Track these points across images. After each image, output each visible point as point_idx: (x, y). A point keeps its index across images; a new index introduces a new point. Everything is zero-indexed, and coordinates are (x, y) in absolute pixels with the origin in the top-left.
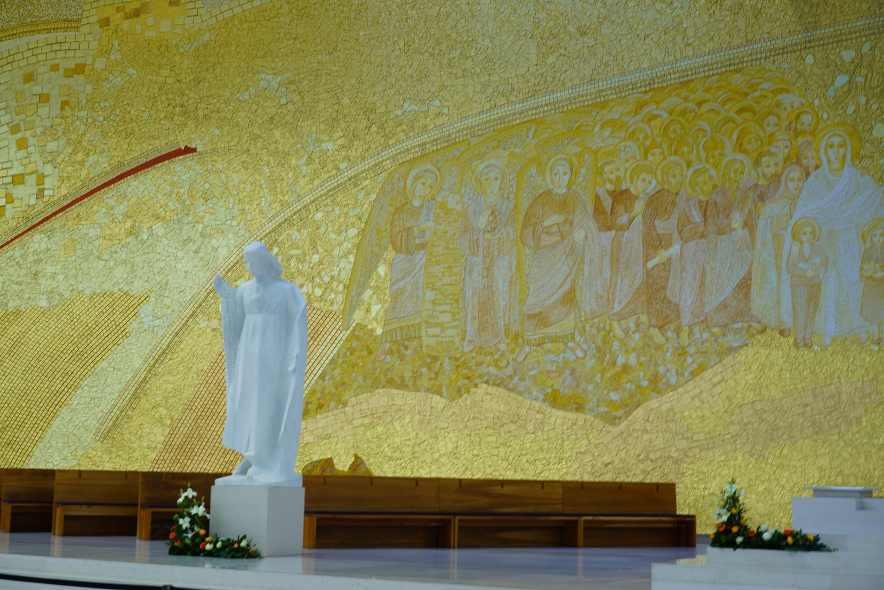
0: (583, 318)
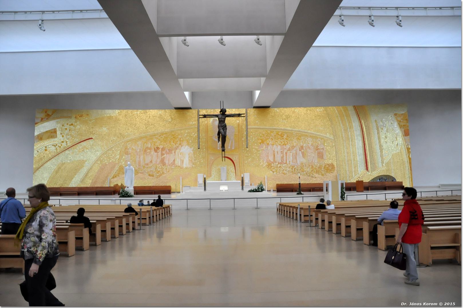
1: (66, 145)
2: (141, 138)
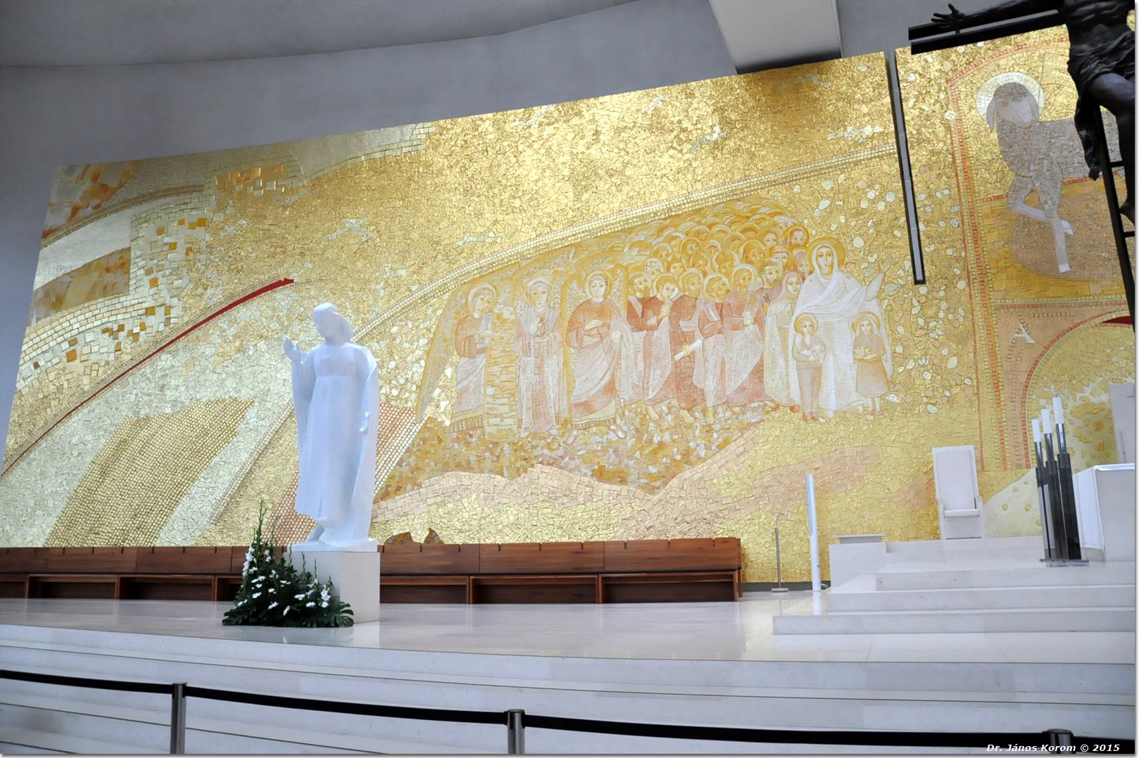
0: (622, 405)
1: (161, 328)
2: (546, 256)
